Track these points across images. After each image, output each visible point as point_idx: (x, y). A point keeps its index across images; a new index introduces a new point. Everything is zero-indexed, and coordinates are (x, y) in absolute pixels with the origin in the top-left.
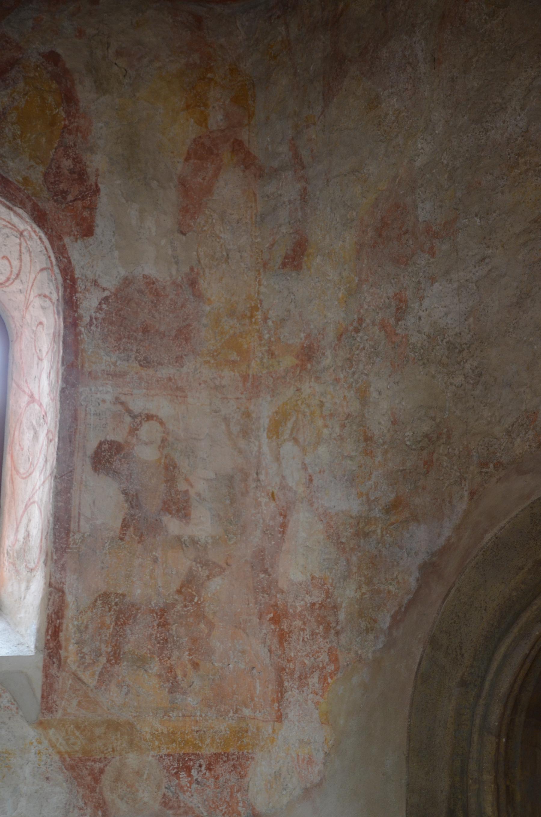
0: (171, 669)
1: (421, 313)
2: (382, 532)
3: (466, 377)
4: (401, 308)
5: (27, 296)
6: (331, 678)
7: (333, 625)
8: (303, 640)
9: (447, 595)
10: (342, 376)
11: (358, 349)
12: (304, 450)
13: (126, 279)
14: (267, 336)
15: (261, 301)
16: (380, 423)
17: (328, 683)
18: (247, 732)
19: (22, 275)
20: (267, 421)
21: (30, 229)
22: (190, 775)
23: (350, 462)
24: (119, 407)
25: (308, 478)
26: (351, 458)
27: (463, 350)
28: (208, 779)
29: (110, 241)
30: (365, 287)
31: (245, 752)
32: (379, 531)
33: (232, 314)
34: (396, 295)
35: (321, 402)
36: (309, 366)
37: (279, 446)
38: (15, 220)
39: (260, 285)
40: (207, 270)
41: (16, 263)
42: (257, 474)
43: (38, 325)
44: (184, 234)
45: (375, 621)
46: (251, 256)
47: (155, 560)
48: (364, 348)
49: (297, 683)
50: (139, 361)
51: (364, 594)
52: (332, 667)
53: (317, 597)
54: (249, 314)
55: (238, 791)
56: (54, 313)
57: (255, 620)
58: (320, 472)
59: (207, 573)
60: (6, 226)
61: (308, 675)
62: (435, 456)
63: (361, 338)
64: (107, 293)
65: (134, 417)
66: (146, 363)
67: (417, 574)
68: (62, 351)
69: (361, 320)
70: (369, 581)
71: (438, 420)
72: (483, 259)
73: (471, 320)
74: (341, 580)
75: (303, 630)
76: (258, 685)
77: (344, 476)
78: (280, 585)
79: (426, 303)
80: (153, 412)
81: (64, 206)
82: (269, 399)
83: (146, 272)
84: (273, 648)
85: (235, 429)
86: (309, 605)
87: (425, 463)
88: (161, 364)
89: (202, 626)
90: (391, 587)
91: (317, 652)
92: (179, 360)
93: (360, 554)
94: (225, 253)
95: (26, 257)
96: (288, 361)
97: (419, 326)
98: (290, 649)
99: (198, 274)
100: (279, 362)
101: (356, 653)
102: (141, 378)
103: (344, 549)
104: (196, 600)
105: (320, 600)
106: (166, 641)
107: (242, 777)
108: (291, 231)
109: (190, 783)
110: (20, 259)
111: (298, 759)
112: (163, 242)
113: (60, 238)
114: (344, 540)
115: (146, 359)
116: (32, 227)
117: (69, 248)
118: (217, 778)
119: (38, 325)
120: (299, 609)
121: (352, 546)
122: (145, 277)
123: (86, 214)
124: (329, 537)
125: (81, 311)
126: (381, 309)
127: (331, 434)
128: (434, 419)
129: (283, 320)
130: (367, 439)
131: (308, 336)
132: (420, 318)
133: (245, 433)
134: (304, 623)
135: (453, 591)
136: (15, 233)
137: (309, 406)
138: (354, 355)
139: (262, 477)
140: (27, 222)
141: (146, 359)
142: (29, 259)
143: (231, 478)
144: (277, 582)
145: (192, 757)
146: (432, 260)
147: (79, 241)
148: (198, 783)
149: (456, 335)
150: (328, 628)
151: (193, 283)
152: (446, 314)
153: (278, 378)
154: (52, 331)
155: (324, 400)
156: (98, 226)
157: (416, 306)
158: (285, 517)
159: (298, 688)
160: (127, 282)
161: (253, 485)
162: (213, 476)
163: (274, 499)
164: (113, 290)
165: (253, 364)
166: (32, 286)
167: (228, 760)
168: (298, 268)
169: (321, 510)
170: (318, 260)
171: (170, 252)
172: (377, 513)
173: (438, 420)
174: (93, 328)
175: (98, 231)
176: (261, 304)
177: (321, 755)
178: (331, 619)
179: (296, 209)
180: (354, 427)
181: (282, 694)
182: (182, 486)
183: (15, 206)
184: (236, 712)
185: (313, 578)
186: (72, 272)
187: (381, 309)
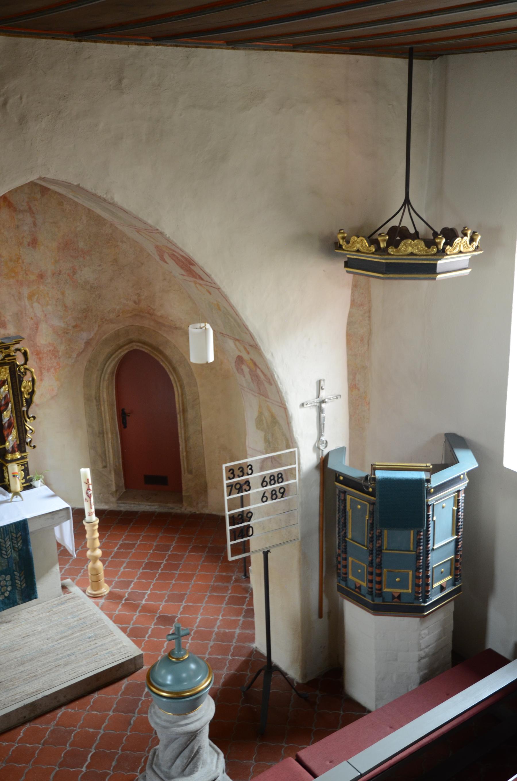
11: (60, 280)
14: (24, 268)
15: (21, 256)
20: (27, 295)
32: (71, 333)
33: (11, 260)
37: (32, 303)
46: (15, 240)
52: (58, 367)
53: (51, 348)
54: (16, 260)
69: (61, 271)
71: (88, 305)
72: (100, 265)
73: (97, 281)
120: (45, 352)
128: (87, 305)
129: (30, 264)
131: (41, 271)
132: (81, 276)
134: (47, 355)
137: (43, 293)
139: (27, 312)
143: (17, 314)
150: (56, 357)
158: (37, 325)
165: (20, 276)
168: (34, 247)
172: (70, 327)
185: (49, 343)
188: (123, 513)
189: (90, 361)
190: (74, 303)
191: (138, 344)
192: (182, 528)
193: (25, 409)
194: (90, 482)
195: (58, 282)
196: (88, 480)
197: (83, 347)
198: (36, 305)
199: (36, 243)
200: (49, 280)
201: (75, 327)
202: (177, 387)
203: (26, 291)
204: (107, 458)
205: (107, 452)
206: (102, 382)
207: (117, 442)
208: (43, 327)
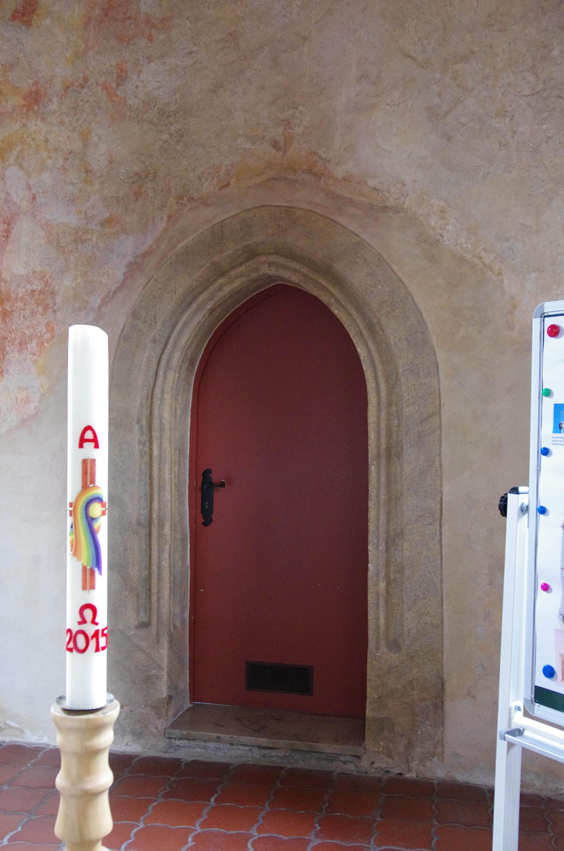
1: (138, 83)
2: (97, 239)
3: (171, 135)
4: (122, 76)
6: (48, 343)
7: (52, 305)
8: (24, 317)
9: (147, 284)
11: (82, 101)
16: (99, 161)
17: (45, 347)
23: (72, 187)
25: (31, 196)
26: (73, 184)
27: (171, 116)
32: (94, 239)
34: (118, 65)
35: (46, 138)
36: (36, 108)
48: (87, 102)
49: (17, 348)
51: (78, 283)
53: (37, 286)
58: (43, 193)
61: (28, 342)
62: (143, 189)
63: (86, 93)
67: (124, 270)
69: (86, 79)
71: (147, 164)
72: (191, 53)
73: (178, 95)
74: (60, 274)
75: (24, 309)
79: (143, 76)
86: (29, 291)
87: (135, 193)
90: (102, 279)
91: (37, 325)
93: (77, 255)
96: (17, 100)
97: (136, 93)
98: (12, 323)
100: (6, 100)
103: (63, 252)
105: (40, 288)
111: (16, 400)
114: (63, 245)
120: (21, 294)
121: (70, 249)
124: (50, 242)
126: (104, 73)
127: (54, 164)
128: (144, 163)
129: (12, 65)
131: (35, 83)
132: (137, 87)
134: (25, 305)
135: (152, 281)
137: (34, 140)
138: (78, 105)
146: (150, 44)
149: (165, 104)
150: (46, 308)
152: (159, 88)
155: (49, 137)
157: (135, 77)
158: (9, 225)
159: (18, 351)
168: (28, 23)
169: (43, 222)
170: (48, 21)
173: (147, 164)
177: (38, 396)
178: (49, 301)
180: (77, 161)
185: (34, 272)
187: (104, 73)
188: (183, 767)
189: (135, 315)
190: (111, 162)
191: (273, 258)
192: (379, 819)
197: (120, 275)
199: (33, 12)
200: (54, 106)
201: (107, 222)
202: (376, 378)
204: (154, 598)
205: (154, 581)
206: (161, 373)
207: (183, 558)
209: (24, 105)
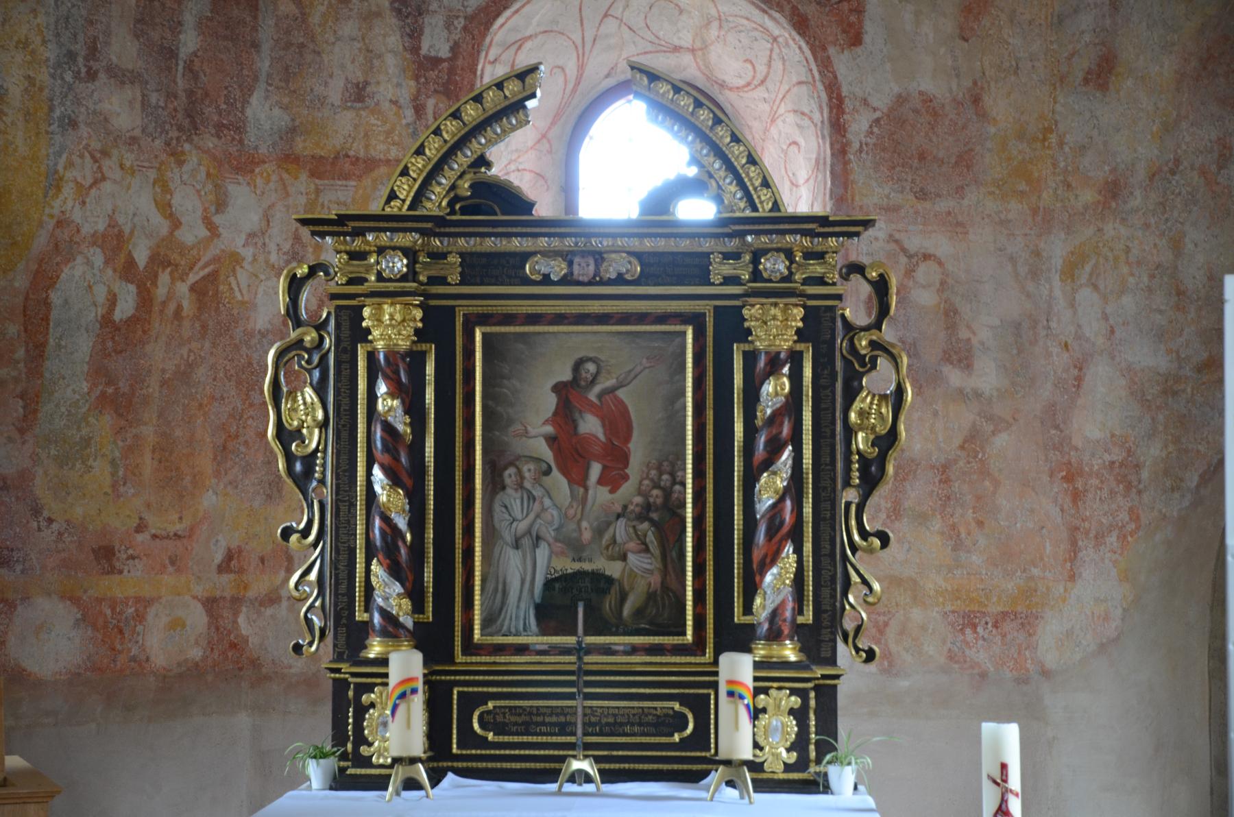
0: (953, 527)
4: (1225, 155)
5: (775, 108)
6: (1132, 536)
7: (1135, 483)
10: (1153, 221)
11: (1173, 194)
12: (1105, 298)
13: (900, 96)
14: (1062, 164)
15: (1056, 122)
16: (1194, 278)
18: (1036, 591)
19: (768, 83)
20: (1060, 262)
21: (787, 35)
22: (975, 632)
23: (1160, 317)
24: (893, 246)
25: (1109, 329)
26: (1161, 312)
28: (995, 636)
29: (881, 51)
30: (1184, 125)
31: (1034, 611)
32: (1189, 390)
33: (1021, 136)
34: (1219, 139)
35: (1128, 247)
36: (1114, 205)
37: (1074, 291)
38: (769, 24)
39: (1055, 103)
40: (992, 84)
41: (762, 69)
42: (1048, 321)
43: (790, 144)
44: (966, 40)
45: (1182, 480)
46: (1045, 67)
47: (935, 414)
48: (1180, 194)
50: (915, 193)
51: (1170, 453)
53: (1117, 455)
54: (1041, 137)
55: (1026, 649)
56: (817, 137)
57: (1046, 478)
58: (1124, 324)
59: (992, 428)
60: (756, 29)
63: (1177, 182)
64: (878, 114)
65: (910, 257)
66: (922, 195)
68: (829, 183)
69: (1177, 161)
70: (1177, 440)
74: (1146, 439)
75: (1101, 489)
76: (1048, 544)
77: (1152, 330)
78: (1074, 442)
80: (931, 251)
81: (827, 9)
82: (1063, 236)
83: (922, 89)
84: (1066, 507)
85: (1023, 270)
88: (939, 196)
89: (987, 483)
90: (1200, 447)
91: (1117, 511)
92: (960, 191)
93: (1167, 413)
94: (1014, 63)
95: (778, 65)
96: (1088, 196)
99: (982, 88)
100: (1077, 196)
101: (1160, 511)
102: (917, 213)
103: (1149, 407)
104: (980, 456)
105: (1120, 458)
106: (949, 498)
107: (1030, 635)
108: (1097, 41)
109: (976, 639)
110: (769, 66)
111: (1093, 617)
112: (942, 50)
113: (824, 49)
114: (1149, 398)
115: (922, 190)
116: (790, 35)
117: (835, 60)
118: (1004, 636)
119: (790, 144)
120: (1096, 467)
121: (1158, 404)
122: (921, 93)
123: (853, 18)
124: (1132, 394)
125: (849, 136)
126: (1201, 152)
127: (1137, 284)
130: (1180, 293)
131: (1114, 170)
133: (1035, 274)
134: (1102, 482)
136: (766, 37)
138: (1167, 200)
139: (1053, 325)
140: (784, 28)
141: (922, 190)
142: (781, 67)
143: (1018, 326)
144: (1071, 439)
145: (978, 615)
147: (845, 52)
148: (984, 639)
150: (1129, 487)
151: (976, 100)
153: (1075, 214)
154: (814, 156)
155: (1131, 245)
156: (866, 33)
158: (1080, 369)
160: (901, 100)
161: (1043, 333)
162: (997, 322)
163: (1068, 350)
164: (885, 110)
165: (1044, 195)
166: (784, 97)
167: (1016, 618)
168: (1103, 87)
170: (1129, 83)
171: (950, 63)
172: (1187, 371)
174: (864, 155)
175: (867, 39)
176: (1056, 125)
177: (1119, 612)
178: (1133, 478)
179: (1104, 16)
180: (1166, 279)
181: (1075, 553)
182: (964, 334)
183: (771, 9)
184: (1025, 570)
185: (1113, 436)
186: (839, 88)
187: (1201, 152)
193: (851, 495)
194: (1015, 782)
195: (1162, 204)
196: (1004, 767)
198: (1085, 295)
200: (1137, 201)
203: (1057, 249)
208: (1101, 375)
209: (1099, 202)
